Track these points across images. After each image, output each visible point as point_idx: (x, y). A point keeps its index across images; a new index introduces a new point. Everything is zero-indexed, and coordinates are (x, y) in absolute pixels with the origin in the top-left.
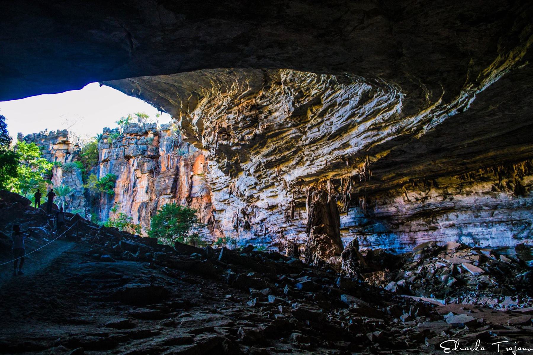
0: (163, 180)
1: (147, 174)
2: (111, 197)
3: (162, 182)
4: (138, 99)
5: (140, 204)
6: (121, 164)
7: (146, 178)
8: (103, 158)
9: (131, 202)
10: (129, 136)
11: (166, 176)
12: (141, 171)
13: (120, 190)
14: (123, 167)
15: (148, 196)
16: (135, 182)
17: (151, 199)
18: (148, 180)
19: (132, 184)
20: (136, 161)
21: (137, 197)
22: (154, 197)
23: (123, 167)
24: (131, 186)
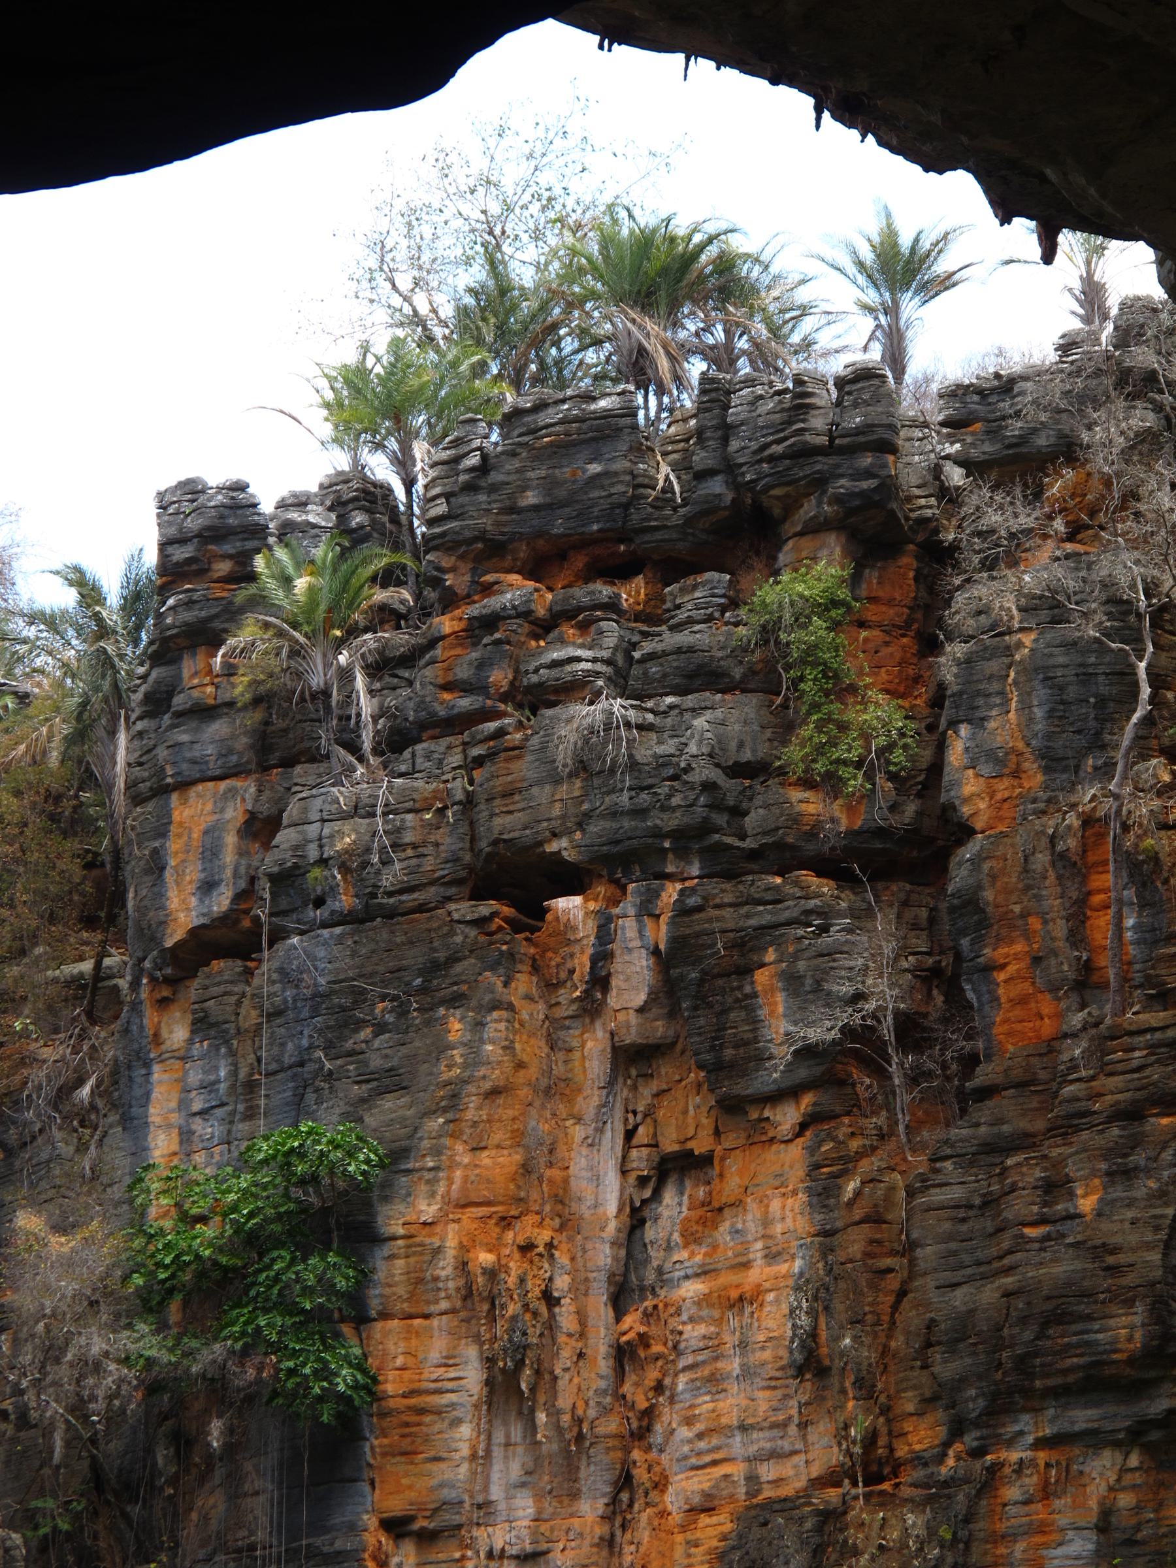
0: (1027, 1172)
1: (787, 1116)
2: (332, 1444)
3: (1023, 1205)
4: (762, 84)
5: (715, 1528)
6: (435, 986)
7: (792, 1159)
8: (184, 910)
9: (590, 1509)
10: (515, 590)
11: (1068, 1126)
12: (717, 1070)
13: (436, 1349)
14: (456, 1027)
15: (821, 1436)
16: (636, 1218)
17: (873, 1467)
18: (823, 1191)
19: (603, 1255)
20: (628, 928)
21: (677, 1435)
22: (921, 1435)
23: (456, 1027)
24: (580, 1288)
